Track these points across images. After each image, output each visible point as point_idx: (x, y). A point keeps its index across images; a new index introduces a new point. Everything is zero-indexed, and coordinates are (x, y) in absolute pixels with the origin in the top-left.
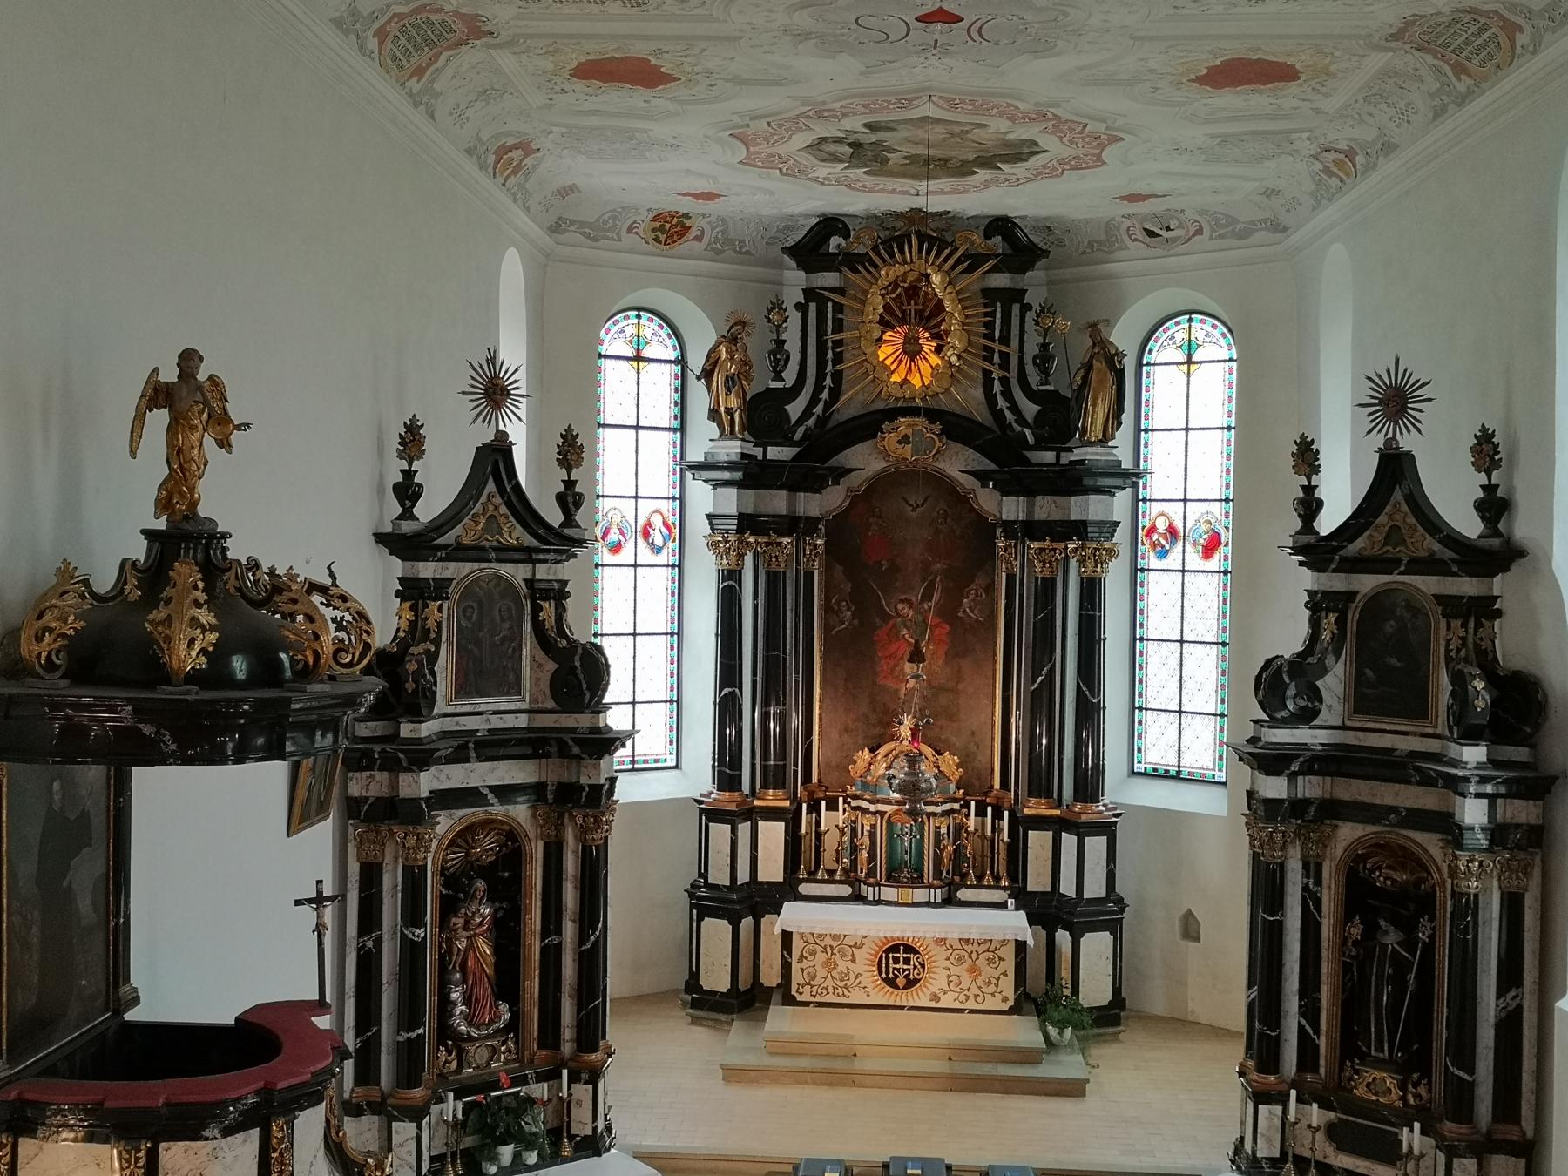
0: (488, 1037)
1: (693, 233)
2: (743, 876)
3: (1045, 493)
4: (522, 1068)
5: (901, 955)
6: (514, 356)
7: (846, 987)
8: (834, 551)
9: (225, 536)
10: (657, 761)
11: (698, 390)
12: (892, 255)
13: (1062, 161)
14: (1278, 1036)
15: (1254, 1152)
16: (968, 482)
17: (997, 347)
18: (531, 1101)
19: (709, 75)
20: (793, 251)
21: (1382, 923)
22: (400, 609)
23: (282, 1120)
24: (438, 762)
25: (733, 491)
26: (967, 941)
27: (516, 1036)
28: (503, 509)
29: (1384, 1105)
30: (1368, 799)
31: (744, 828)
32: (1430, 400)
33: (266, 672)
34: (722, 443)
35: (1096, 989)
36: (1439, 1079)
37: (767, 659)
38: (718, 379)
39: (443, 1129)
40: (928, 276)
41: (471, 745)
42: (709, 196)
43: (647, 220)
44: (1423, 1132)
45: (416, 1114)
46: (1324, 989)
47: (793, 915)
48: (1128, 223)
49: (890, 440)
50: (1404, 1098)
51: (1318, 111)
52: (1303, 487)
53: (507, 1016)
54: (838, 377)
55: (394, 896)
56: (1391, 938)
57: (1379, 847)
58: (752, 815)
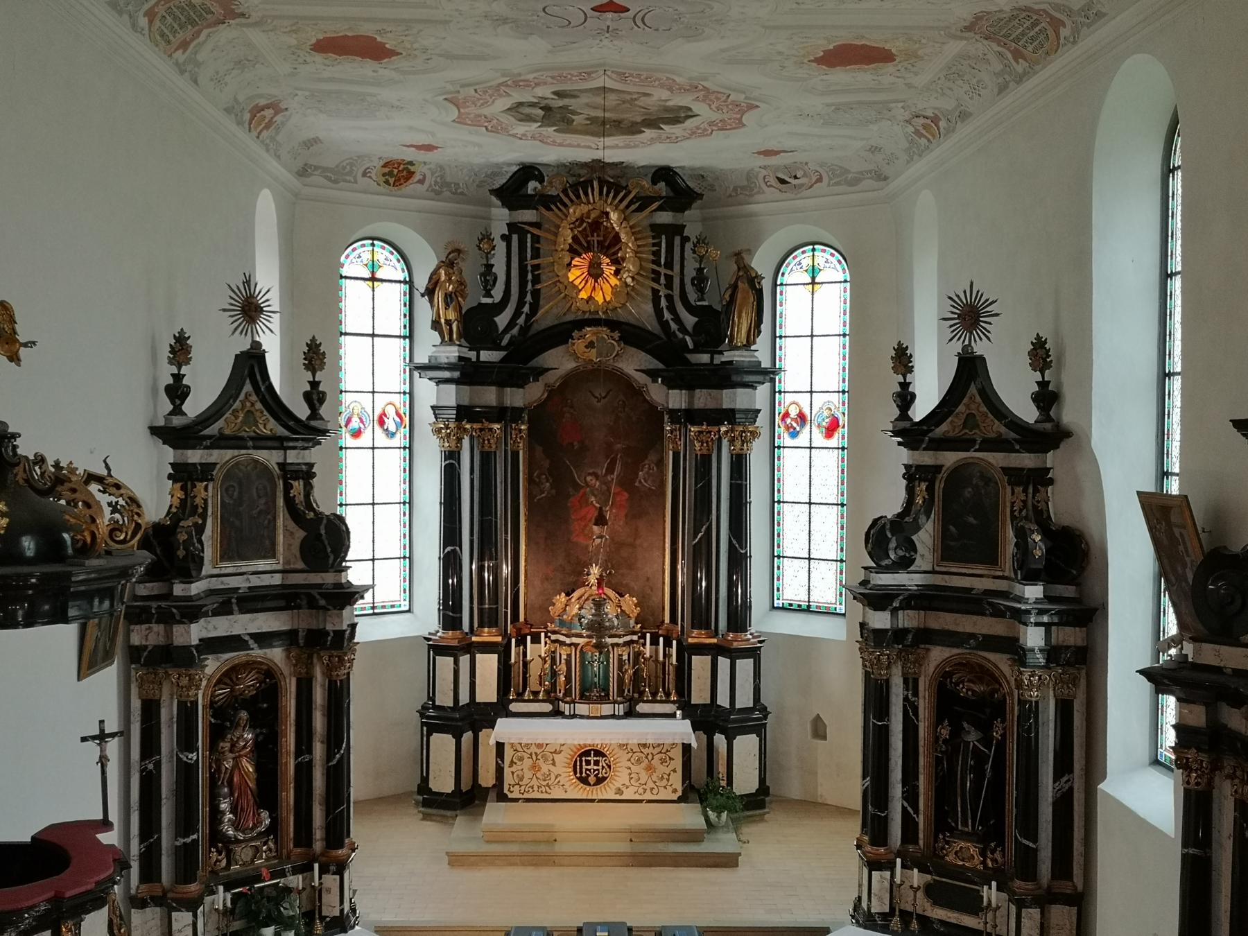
0: (252, 839)
1: (417, 177)
2: (464, 699)
3: (702, 387)
4: (281, 864)
5: (592, 759)
6: (268, 283)
7: (548, 785)
9: (15, 436)
10: (393, 606)
11: (422, 304)
12: (578, 197)
13: (711, 124)
14: (886, 817)
15: (869, 908)
16: (642, 378)
17: (663, 271)
18: (288, 890)
19: (425, 50)
20: (500, 193)
21: (965, 725)
22: (172, 489)
23: (70, 923)
24: (206, 615)
25: (452, 387)
26: (644, 745)
27: (276, 837)
28: (259, 406)
29: (968, 869)
30: (952, 628)
31: (465, 660)
32: (997, 315)
33: (51, 549)
34: (443, 348)
35: (746, 780)
36: (1011, 847)
37: (481, 523)
38: (439, 296)
39: (215, 917)
40: (607, 214)
41: (234, 601)
42: (429, 148)
43: (378, 167)
44: (998, 889)
45: (192, 905)
46: (921, 778)
47: (505, 729)
48: (764, 172)
49: (579, 345)
50: (984, 863)
51: (909, 86)
52: (900, 384)
53: (267, 822)
54: (536, 294)
55: (170, 726)
56: (973, 737)
57: (963, 665)
58: (471, 649)
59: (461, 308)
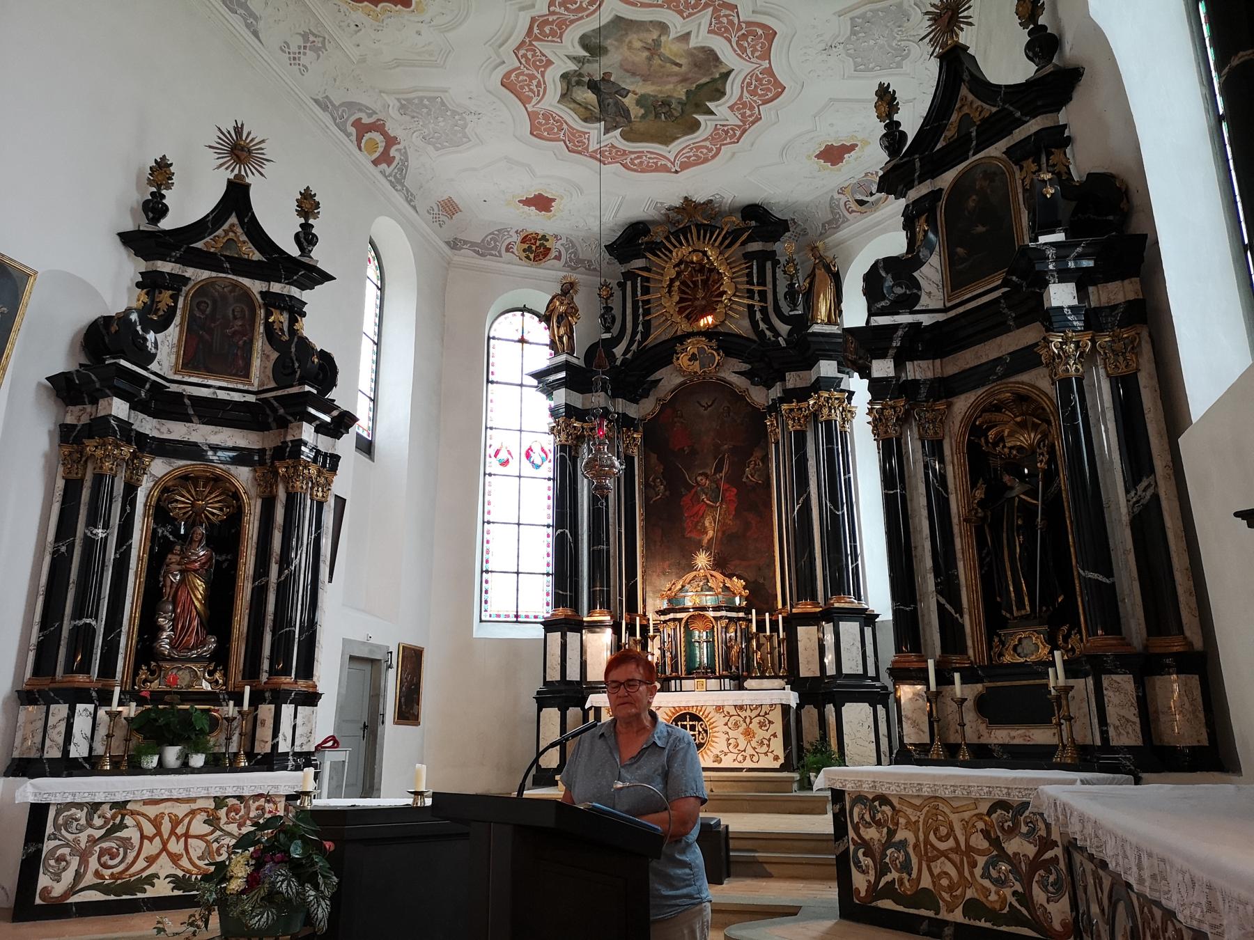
1: (553, 254)
5: (688, 723)
8: (650, 444)
12: (681, 244)
16: (739, 381)
17: (756, 288)
26: (741, 708)
28: (244, 238)
31: (573, 638)
45: (75, 696)
46: (960, 565)
48: (843, 199)
49: (683, 360)
53: (213, 646)
54: (647, 325)
59: (571, 326)
